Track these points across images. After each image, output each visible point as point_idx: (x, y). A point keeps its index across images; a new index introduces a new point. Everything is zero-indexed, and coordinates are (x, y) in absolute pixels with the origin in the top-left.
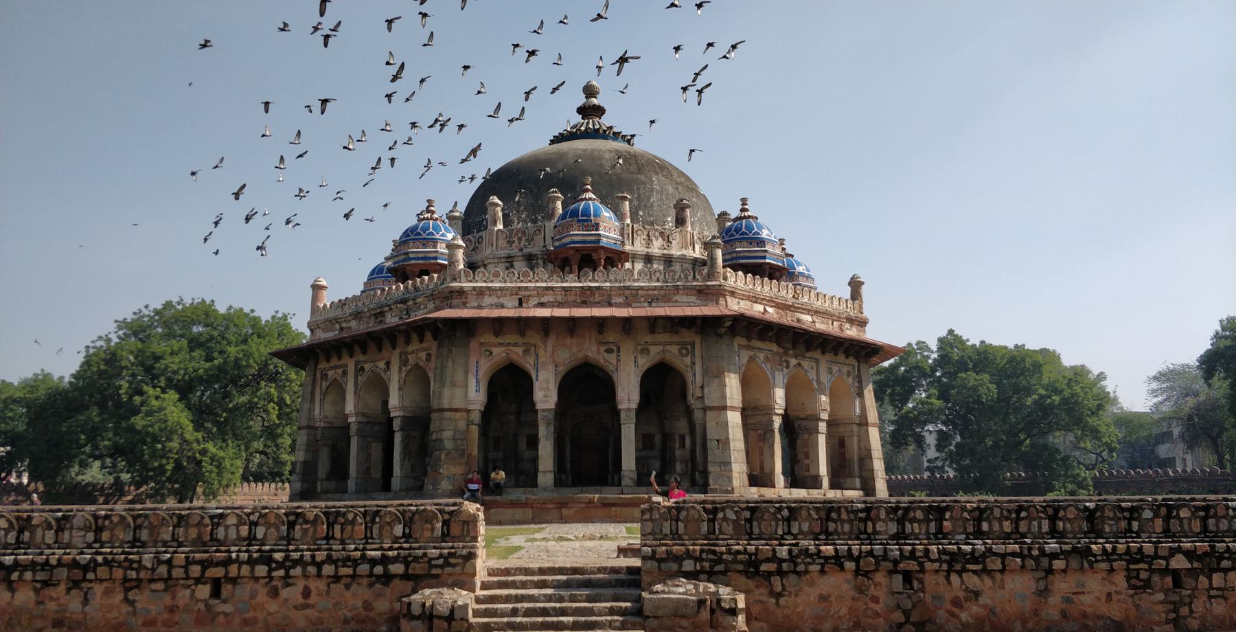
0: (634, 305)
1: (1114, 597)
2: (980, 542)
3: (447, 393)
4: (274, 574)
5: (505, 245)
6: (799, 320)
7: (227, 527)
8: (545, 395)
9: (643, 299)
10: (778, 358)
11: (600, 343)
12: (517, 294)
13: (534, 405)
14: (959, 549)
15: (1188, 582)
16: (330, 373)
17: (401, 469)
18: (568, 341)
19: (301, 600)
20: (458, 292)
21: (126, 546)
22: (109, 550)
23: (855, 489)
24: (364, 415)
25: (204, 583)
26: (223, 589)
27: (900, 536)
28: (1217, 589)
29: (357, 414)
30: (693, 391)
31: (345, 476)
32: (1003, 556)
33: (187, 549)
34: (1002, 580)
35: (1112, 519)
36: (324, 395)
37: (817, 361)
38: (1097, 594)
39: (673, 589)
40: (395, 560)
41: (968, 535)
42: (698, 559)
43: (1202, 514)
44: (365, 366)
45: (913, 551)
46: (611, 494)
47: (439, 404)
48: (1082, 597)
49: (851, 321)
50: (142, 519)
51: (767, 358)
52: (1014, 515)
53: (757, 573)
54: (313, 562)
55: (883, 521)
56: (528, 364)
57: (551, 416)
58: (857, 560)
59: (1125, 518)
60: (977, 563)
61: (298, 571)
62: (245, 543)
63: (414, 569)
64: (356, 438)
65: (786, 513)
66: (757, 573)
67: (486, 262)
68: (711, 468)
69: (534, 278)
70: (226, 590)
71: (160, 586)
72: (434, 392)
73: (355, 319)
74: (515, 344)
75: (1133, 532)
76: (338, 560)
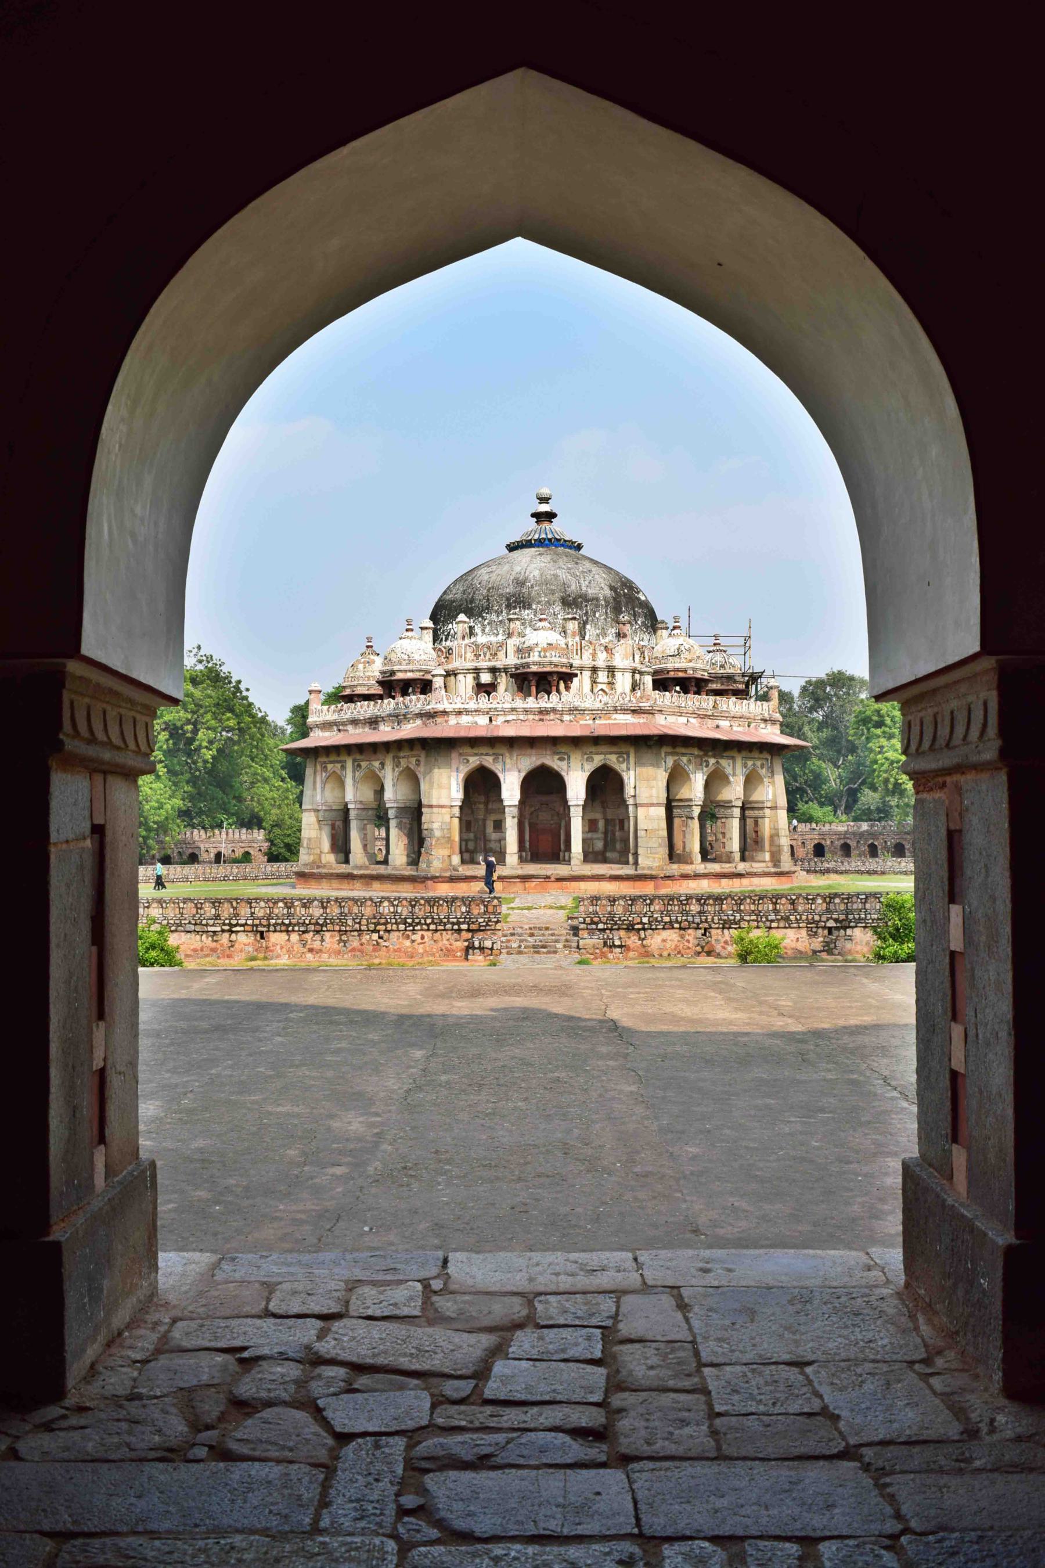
0: (582, 722)
3: (435, 793)
6: (718, 727)
8: (511, 791)
10: (699, 760)
12: (488, 713)
13: (501, 801)
15: (835, 933)
16: (330, 766)
18: (529, 751)
19: (420, 941)
24: (361, 802)
27: (701, 913)
32: (749, 921)
36: (324, 783)
37: (733, 758)
40: (464, 923)
46: (561, 870)
49: (765, 721)
51: (689, 761)
53: (633, 929)
54: (426, 924)
56: (497, 768)
57: (515, 811)
58: (680, 923)
61: (419, 927)
65: (648, 902)
66: (633, 929)
68: (640, 851)
71: (356, 933)
74: (487, 754)
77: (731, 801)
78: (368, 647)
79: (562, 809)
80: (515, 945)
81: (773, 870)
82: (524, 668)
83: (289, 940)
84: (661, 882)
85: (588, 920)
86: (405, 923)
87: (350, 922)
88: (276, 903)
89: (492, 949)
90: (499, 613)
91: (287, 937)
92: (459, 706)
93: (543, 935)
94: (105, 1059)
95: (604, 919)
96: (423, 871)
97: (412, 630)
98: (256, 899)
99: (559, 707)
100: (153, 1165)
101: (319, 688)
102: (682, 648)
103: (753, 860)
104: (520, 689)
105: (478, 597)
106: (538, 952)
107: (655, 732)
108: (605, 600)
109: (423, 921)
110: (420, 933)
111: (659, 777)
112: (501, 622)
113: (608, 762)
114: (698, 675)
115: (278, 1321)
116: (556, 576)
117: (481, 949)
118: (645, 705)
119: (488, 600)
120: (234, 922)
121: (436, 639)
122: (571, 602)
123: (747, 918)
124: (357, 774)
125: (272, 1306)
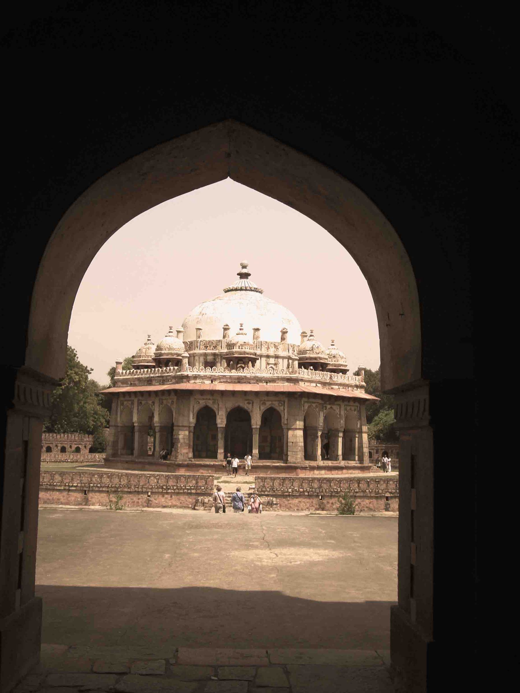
0: (260, 384)
2: (339, 489)
3: (181, 419)
6: (332, 388)
7: (151, 480)
8: (221, 421)
9: (264, 382)
13: (216, 424)
14: (334, 491)
16: (125, 403)
17: (159, 448)
20: (185, 376)
23: (355, 460)
29: (139, 422)
31: (132, 449)
35: (372, 484)
36: (121, 412)
37: (340, 405)
38: (367, 502)
40: (193, 489)
41: (337, 487)
43: (396, 483)
49: (357, 386)
52: (349, 483)
55: (316, 483)
56: (215, 407)
58: (308, 492)
60: (338, 494)
61: (169, 491)
64: (138, 433)
65: (292, 480)
67: (194, 355)
68: (289, 453)
69: (218, 371)
72: (175, 418)
73: (138, 380)
74: (209, 399)
77: (338, 429)
78: (148, 340)
81: (359, 465)
82: (231, 354)
84: (299, 471)
86: (162, 488)
88: (93, 475)
94: (23, 549)
96: (173, 461)
97: (172, 332)
98: (81, 473)
99: (248, 375)
100: (40, 600)
102: (314, 346)
104: (228, 365)
107: (299, 390)
113: (273, 406)
115: (97, 675)
117: (203, 504)
120: (71, 484)
124: (140, 408)
125: (94, 669)
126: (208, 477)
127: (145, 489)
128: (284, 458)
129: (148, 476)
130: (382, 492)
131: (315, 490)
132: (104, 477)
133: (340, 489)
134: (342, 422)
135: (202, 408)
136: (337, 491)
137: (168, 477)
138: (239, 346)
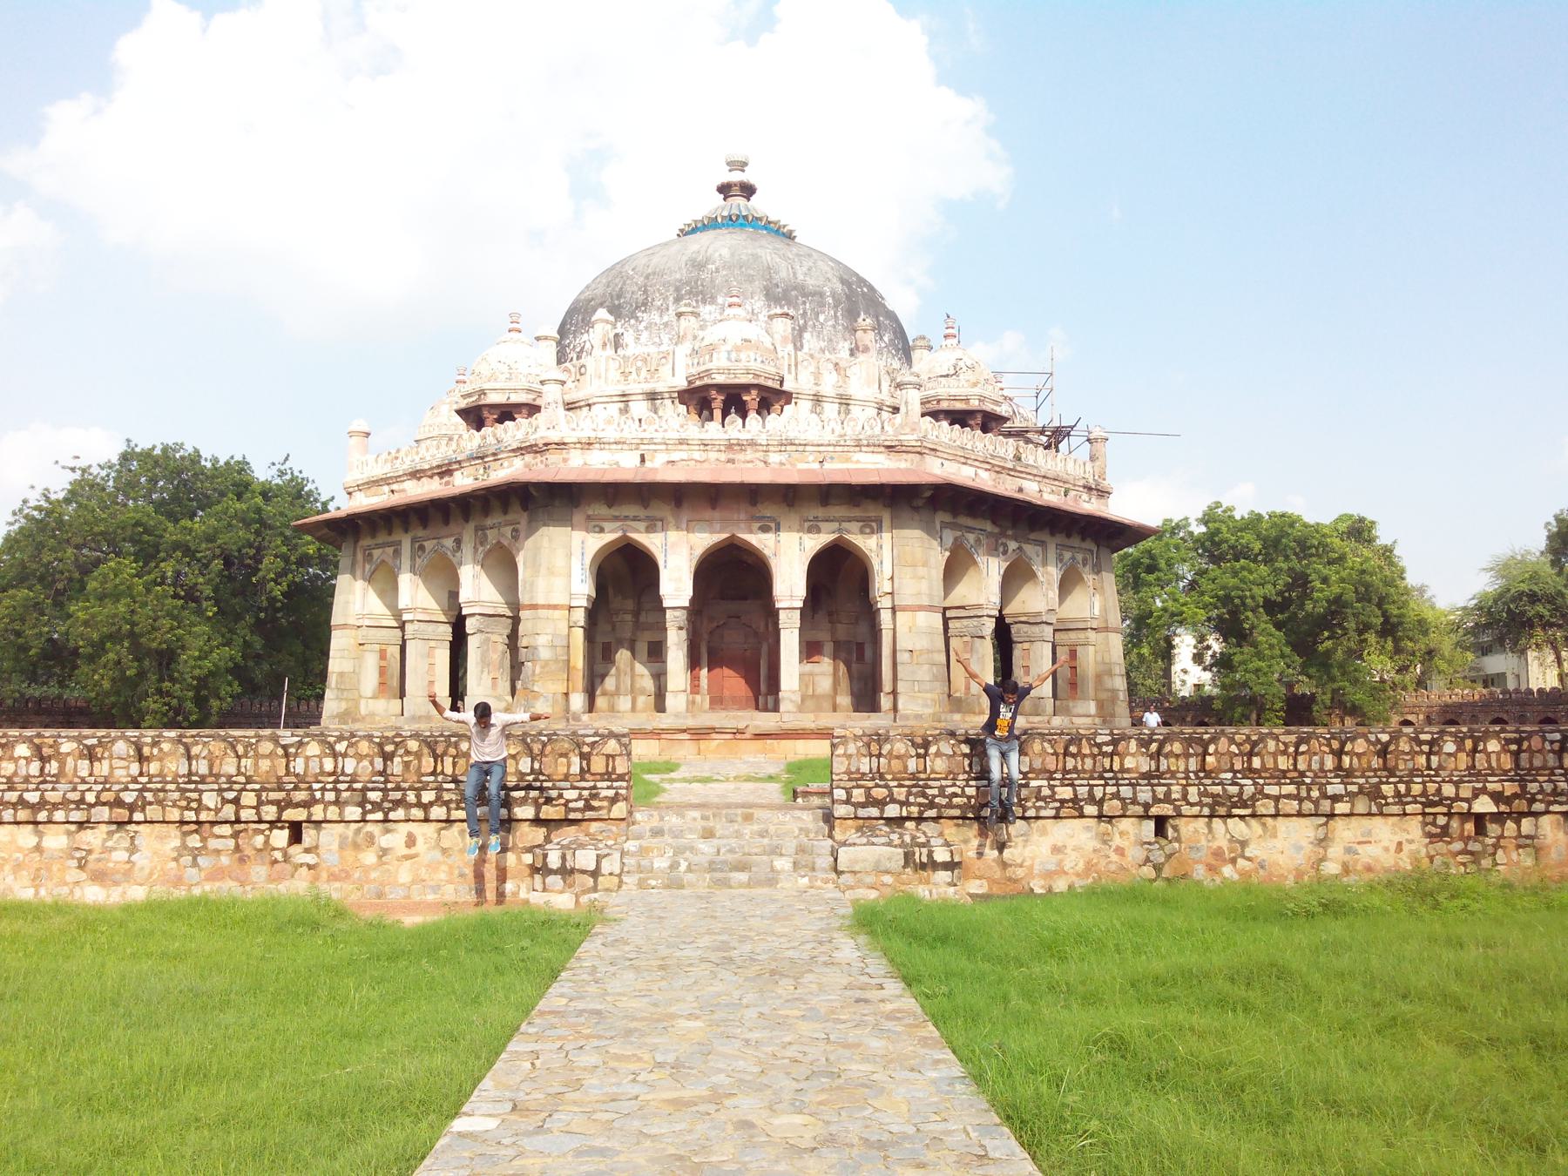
1: (1406, 847)
3: (541, 583)
4: (370, 817)
5: (618, 376)
6: (1021, 490)
7: (307, 759)
9: (811, 458)
11: (754, 518)
13: (659, 600)
14: (1224, 790)
15: (1493, 829)
16: (376, 553)
18: (708, 514)
19: (406, 851)
21: (180, 780)
22: (159, 786)
25: (282, 828)
26: (304, 836)
28: (1527, 837)
30: (881, 585)
32: (1277, 799)
33: (257, 787)
34: (1275, 827)
35: (1407, 754)
37: (1042, 544)
38: (1386, 843)
39: (875, 840)
40: (523, 801)
41: (1235, 772)
42: (902, 804)
43: (1514, 747)
44: (425, 544)
45: (1168, 794)
46: (766, 721)
47: (532, 598)
48: (1368, 848)
50: (200, 747)
51: (978, 541)
52: (1292, 749)
55: (1133, 755)
57: (682, 616)
58: (1100, 803)
59: (1422, 752)
60: (1245, 806)
61: (399, 814)
62: (331, 779)
63: (547, 813)
68: (901, 687)
70: (309, 835)
71: (226, 830)
74: (635, 519)
75: (1431, 769)
76: (450, 801)
77: (1039, 614)
79: (762, 625)
80: (661, 863)
82: (701, 378)
83: (38, 848)
85: (859, 795)
87: (210, 799)
89: (595, 874)
90: (663, 311)
91: (33, 841)
92: (585, 433)
93: (738, 834)
95: (900, 794)
99: (762, 439)
101: (367, 430)
102: (961, 364)
103: (1067, 712)
105: (629, 288)
106: (725, 884)
108: (833, 297)
109: (411, 797)
110: (404, 828)
111: (933, 560)
112: (666, 325)
114: (989, 407)
116: (756, 257)
117: (566, 872)
118: (910, 438)
119: (645, 292)
121: (561, 358)
122: (782, 296)
123: (1272, 790)
126: (597, 739)
127: (274, 809)
128: (885, 702)
129: (292, 745)
130: (1457, 794)
131: (1135, 793)
132: (68, 754)
133: (1255, 784)
134: (1054, 594)
135: (611, 555)
136: (1241, 793)
137: (394, 743)
138: (729, 352)
